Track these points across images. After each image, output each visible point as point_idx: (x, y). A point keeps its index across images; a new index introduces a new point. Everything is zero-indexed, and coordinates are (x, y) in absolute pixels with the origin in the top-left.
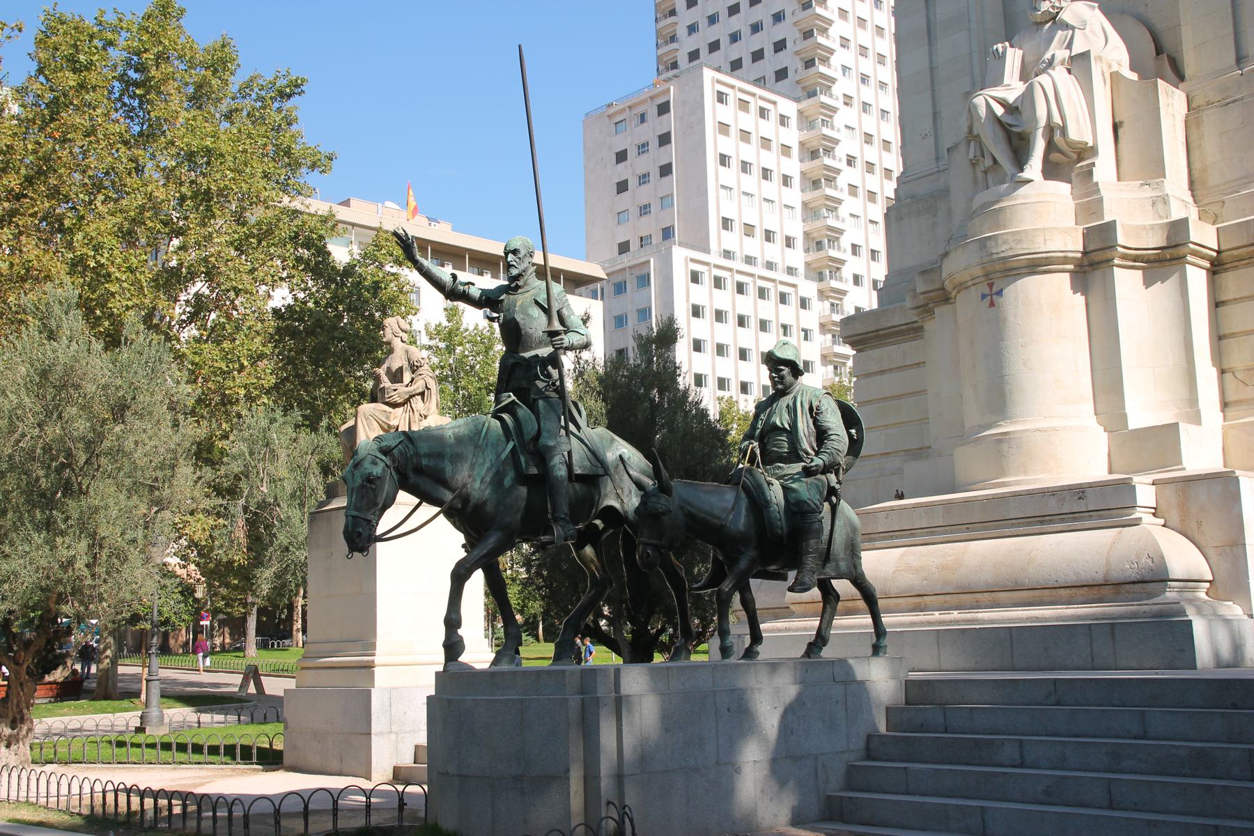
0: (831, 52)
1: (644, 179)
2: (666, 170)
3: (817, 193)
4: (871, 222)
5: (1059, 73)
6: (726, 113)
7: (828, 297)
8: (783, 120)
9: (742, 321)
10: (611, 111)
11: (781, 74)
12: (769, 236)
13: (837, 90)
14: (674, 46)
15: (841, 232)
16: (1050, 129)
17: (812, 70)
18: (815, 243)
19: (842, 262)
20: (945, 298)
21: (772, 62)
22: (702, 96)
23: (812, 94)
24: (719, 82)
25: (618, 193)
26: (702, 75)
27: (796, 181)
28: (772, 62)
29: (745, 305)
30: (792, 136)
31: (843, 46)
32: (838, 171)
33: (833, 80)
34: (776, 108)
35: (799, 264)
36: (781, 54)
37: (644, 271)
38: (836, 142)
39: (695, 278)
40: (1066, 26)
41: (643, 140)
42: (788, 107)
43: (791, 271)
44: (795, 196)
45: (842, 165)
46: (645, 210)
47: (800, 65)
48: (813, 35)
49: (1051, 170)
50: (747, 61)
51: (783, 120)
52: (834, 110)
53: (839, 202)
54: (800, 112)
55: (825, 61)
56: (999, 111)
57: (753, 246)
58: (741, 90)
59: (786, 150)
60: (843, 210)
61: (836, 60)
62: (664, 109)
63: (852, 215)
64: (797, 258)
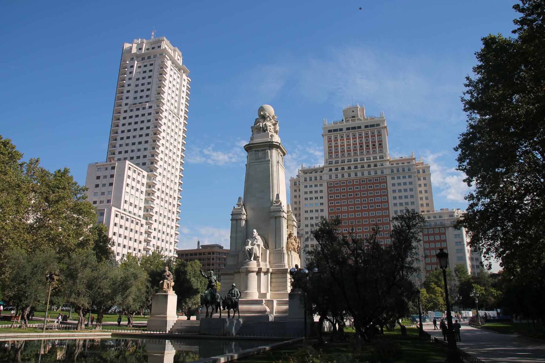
0: (158, 161)
1: (104, 185)
2: (111, 184)
3: (149, 197)
4: (161, 206)
5: (256, 246)
6: (130, 173)
7: (148, 225)
8: (143, 176)
9: (126, 228)
10: (97, 165)
11: (144, 164)
12: (135, 206)
13: (158, 171)
14: (115, 149)
15: (154, 208)
16: (255, 254)
17: (152, 165)
18: (146, 210)
19: (153, 216)
20: (239, 272)
21: (141, 160)
22: (125, 167)
23: (151, 171)
24: (130, 164)
25: (96, 187)
26: (126, 162)
27: (144, 193)
28: (141, 160)
29: (128, 224)
30: (145, 181)
31: (161, 160)
32: (155, 192)
33: (157, 169)
34: (142, 173)
35: (142, 215)
36: (145, 159)
37: (103, 212)
38: (156, 184)
39: (116, 216)
40: (257, 239)
41: (106, 175)
42: (145, 173)
43: (139, 216)
44: (143, 196)
45: (156, 191)
46: (103, 194)
47: (150, 163)
48: (154, 156)
49: (255, 259)
50: (135, 158)
51: (143, 176)
52: (157, 176)
53: (154, 200)
54: (148, 175)
55: (156, 163)
56: (248, 250)
57: (131, 209)
58: (135, 167)
59: (143, 184)
60: (155, 202)
61: (159, 163)
62: (113, 168)
63: (157, 204)
64: (141, 213)
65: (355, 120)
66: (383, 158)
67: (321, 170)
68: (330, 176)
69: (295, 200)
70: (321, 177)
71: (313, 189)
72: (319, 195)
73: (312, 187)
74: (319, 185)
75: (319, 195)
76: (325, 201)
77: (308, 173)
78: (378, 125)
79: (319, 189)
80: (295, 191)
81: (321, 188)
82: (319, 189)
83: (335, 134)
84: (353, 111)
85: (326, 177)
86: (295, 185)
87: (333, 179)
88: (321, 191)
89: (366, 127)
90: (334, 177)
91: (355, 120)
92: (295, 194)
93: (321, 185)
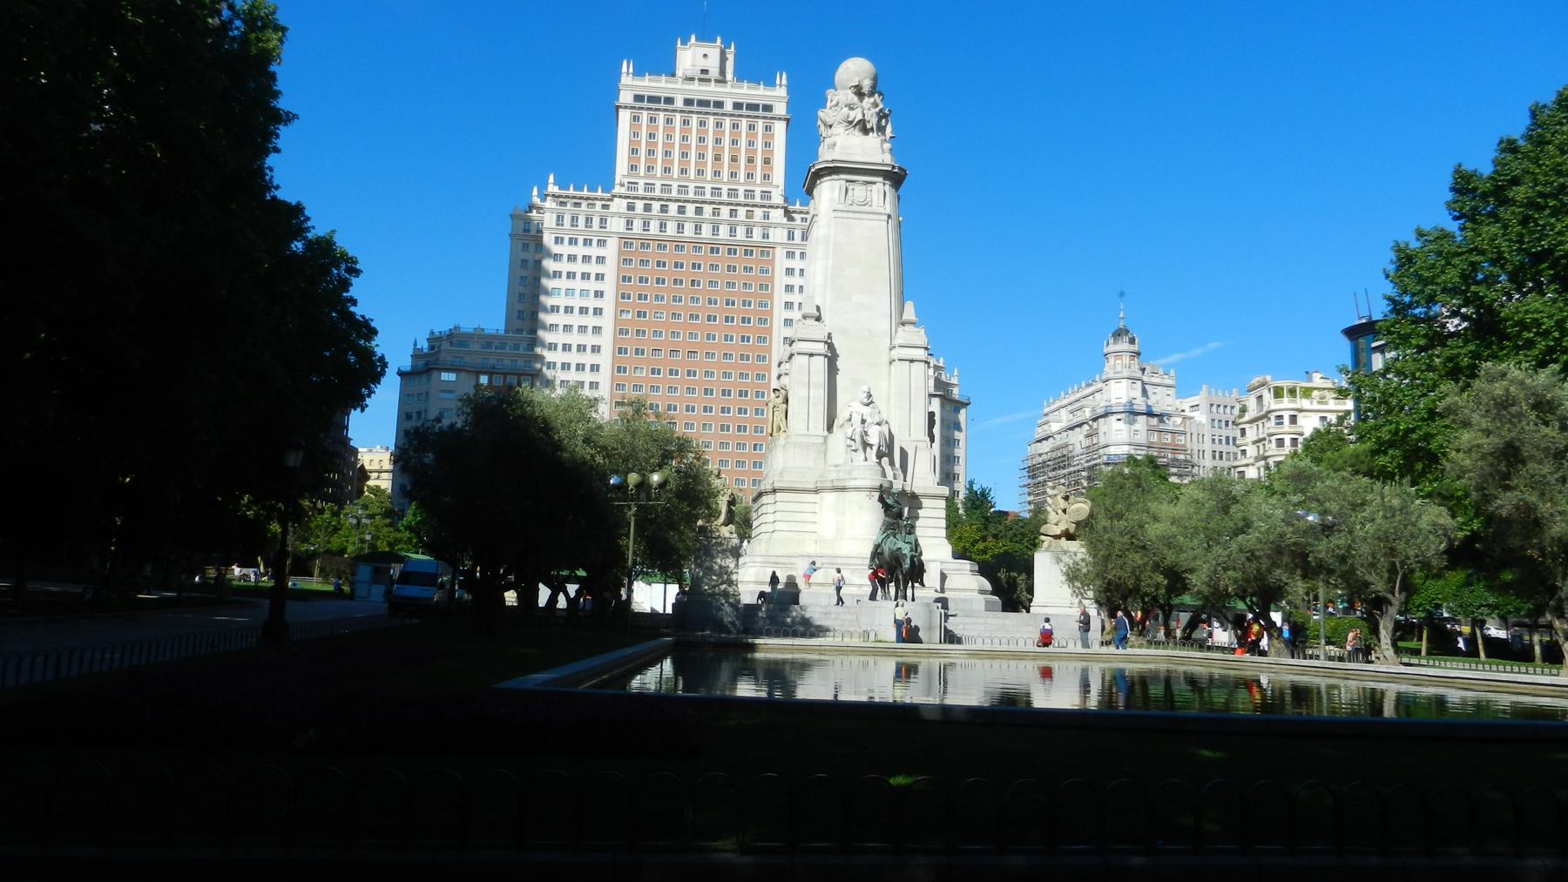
65: (709, 80)
66: (770, 198)
67: (604, 202)
68: (629, 223)
69: (524, 273)
70: (603, 221)
71: (580, 250)
72: (593, 268)
73: (576, 243)
74: (595, 243)
75: (593, 268)
76: (609, 286)
77: (569, 205)
78: (768, 108)
79: (594, 251)
80: (525, 247)
81: (601, 252)
82: (594, 251)
83: (651, 109)
84: (705, 56)
85: (616, 225)
86: (525, 230)
87: (635, 231)
88: (601, 260)
89: (737, 106)
90: (637, 226)
91: (709, 80)
92: (525, 255)
93: (602, 243)
